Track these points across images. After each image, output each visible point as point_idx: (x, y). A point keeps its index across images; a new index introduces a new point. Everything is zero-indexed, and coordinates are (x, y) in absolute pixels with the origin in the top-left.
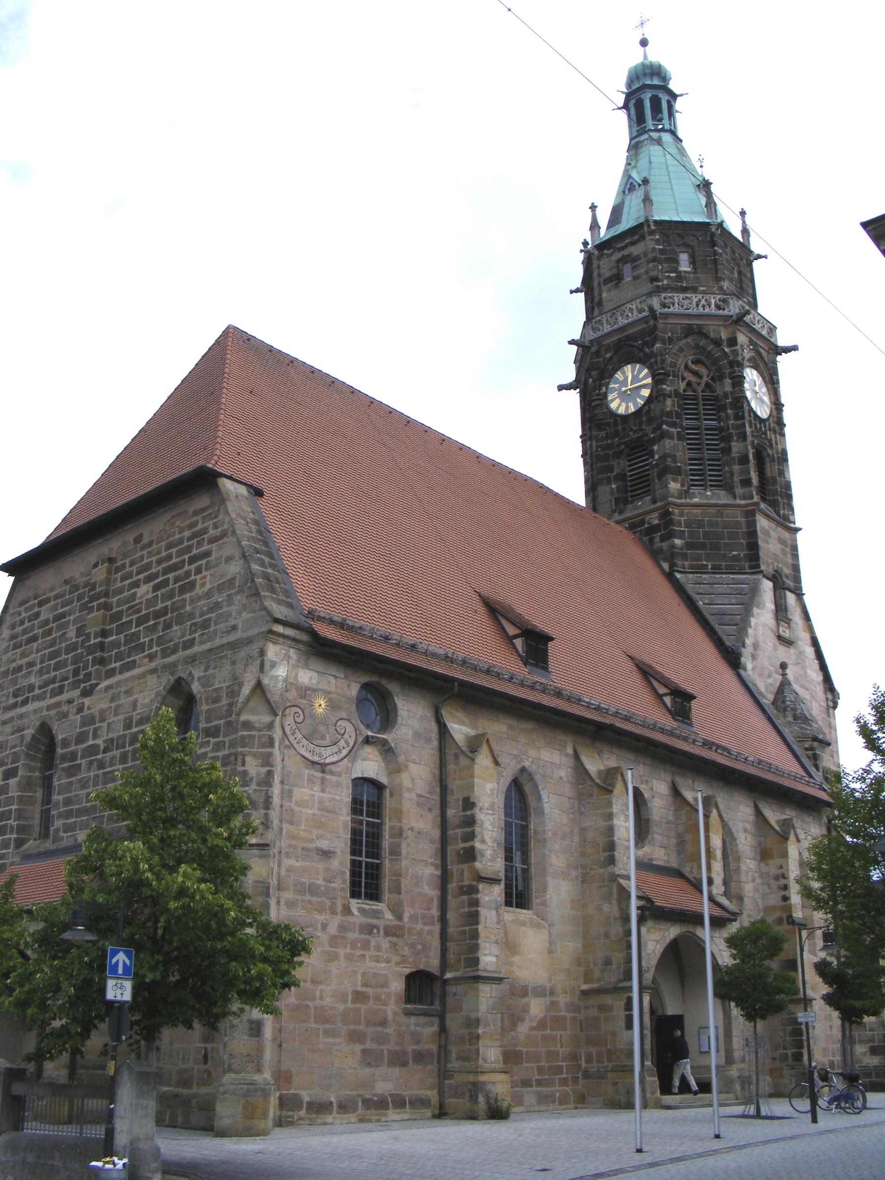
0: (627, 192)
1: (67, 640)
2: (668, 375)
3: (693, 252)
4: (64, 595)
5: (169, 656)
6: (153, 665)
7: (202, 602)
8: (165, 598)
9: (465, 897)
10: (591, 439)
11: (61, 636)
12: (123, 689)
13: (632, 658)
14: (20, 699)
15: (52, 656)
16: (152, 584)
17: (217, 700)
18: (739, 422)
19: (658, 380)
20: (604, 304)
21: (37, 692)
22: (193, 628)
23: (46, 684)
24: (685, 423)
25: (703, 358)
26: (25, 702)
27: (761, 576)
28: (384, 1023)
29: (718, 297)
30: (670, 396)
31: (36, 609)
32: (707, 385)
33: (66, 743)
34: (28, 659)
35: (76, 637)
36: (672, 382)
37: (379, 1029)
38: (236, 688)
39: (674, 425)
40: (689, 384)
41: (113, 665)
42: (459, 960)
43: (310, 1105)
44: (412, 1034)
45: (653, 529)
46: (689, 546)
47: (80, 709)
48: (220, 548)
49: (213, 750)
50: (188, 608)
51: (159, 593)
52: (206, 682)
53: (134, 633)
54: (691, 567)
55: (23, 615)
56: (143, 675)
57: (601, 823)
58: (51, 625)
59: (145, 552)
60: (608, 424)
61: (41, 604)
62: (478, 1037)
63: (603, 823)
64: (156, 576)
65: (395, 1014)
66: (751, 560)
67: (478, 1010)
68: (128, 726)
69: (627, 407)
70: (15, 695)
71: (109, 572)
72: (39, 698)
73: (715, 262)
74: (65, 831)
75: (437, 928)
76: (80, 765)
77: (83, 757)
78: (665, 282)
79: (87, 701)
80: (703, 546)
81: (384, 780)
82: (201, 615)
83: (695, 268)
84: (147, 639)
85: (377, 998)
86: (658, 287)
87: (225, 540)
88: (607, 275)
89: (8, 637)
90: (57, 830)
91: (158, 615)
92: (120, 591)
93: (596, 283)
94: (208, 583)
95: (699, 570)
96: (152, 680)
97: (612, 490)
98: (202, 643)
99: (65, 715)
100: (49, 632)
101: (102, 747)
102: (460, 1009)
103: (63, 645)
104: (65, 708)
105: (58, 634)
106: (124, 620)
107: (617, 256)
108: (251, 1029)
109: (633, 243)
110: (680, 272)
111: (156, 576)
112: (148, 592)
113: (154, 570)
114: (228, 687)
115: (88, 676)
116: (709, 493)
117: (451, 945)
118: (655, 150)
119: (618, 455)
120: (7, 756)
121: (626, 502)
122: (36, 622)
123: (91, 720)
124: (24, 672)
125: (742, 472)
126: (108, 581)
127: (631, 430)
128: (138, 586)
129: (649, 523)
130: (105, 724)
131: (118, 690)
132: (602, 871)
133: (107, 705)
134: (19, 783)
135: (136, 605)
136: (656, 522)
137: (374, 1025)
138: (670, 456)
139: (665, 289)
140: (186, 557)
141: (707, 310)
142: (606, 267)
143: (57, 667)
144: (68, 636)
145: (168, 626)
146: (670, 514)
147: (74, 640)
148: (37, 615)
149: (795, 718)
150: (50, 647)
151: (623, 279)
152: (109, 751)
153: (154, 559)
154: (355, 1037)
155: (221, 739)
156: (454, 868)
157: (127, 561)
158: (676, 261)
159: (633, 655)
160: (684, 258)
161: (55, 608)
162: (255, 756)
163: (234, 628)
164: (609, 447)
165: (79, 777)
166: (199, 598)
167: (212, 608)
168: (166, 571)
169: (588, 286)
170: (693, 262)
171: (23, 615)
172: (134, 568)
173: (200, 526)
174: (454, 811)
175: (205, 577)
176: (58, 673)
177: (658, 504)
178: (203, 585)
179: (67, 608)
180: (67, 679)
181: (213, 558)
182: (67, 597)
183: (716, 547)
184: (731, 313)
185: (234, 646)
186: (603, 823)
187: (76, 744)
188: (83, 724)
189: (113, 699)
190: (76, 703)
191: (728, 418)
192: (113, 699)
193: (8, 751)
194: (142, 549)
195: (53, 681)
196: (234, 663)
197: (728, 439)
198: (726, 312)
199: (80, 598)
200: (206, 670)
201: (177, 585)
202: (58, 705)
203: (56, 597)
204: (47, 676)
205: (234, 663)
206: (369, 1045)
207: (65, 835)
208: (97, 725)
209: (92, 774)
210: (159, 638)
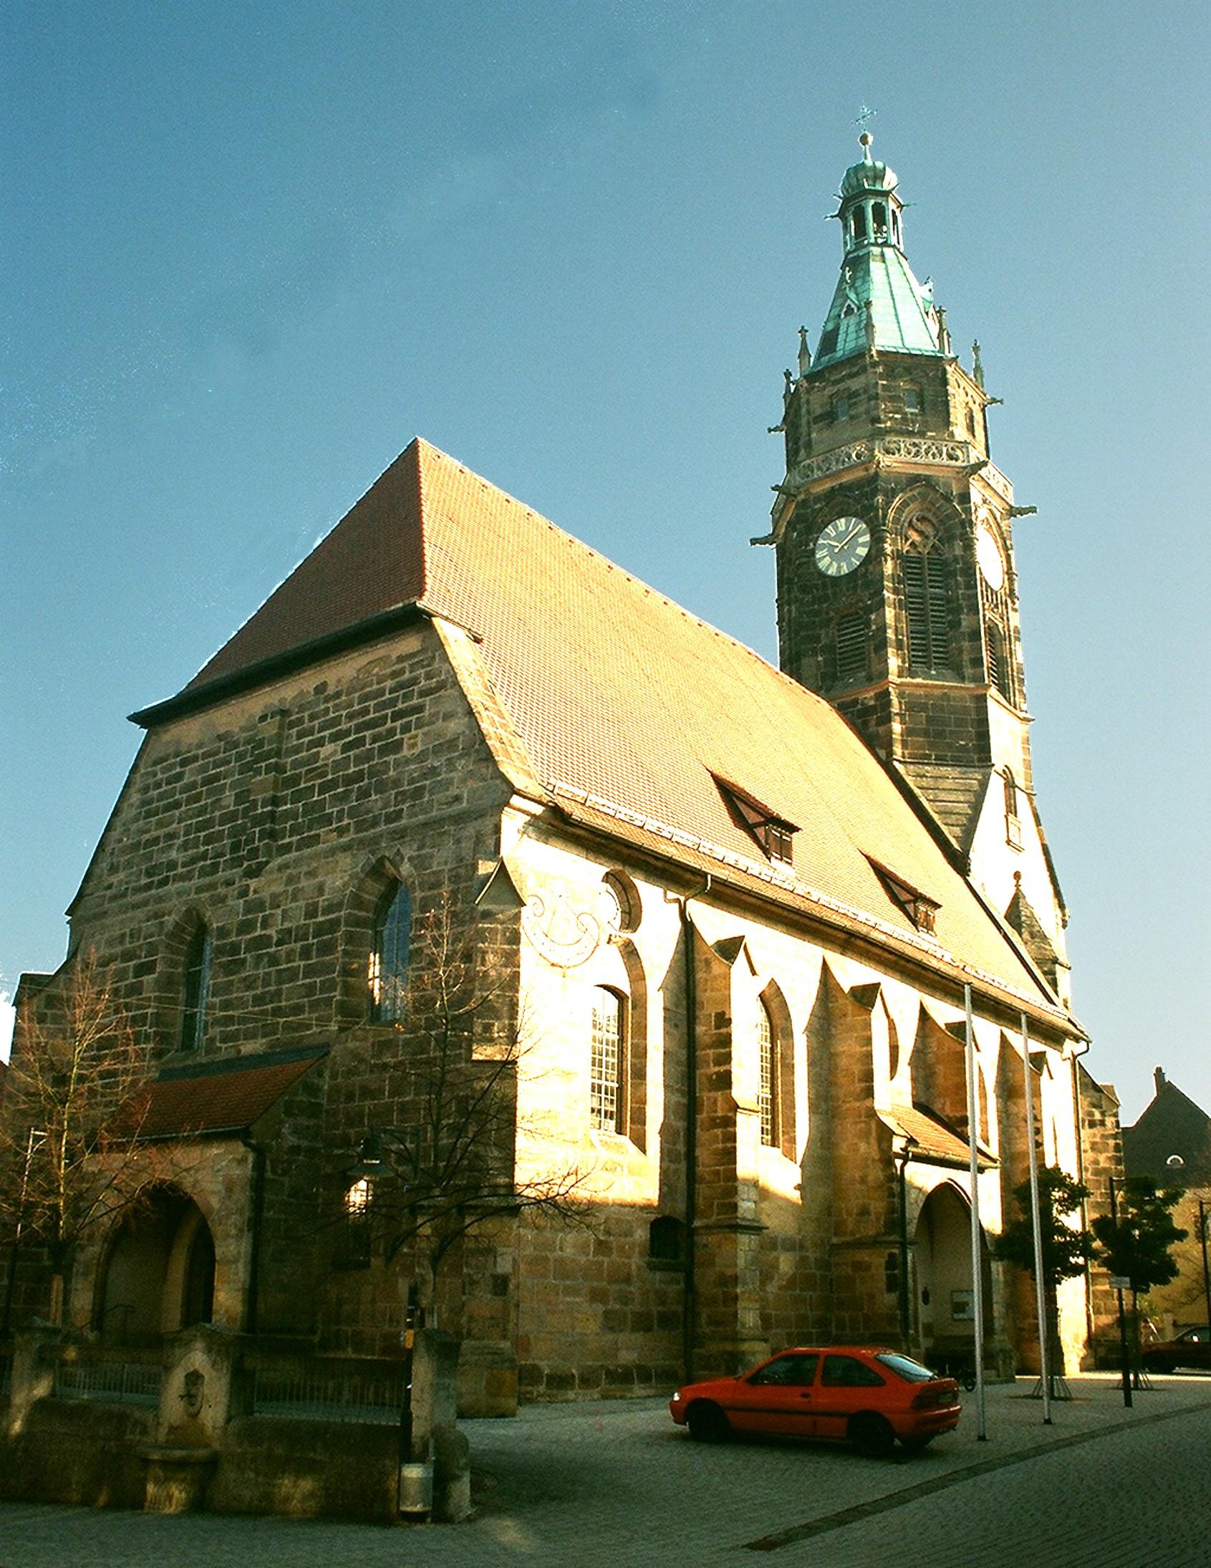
3: (922, 390)
9: (719, 1131)
12: (305, 869)
13: (867, 857)
14: (156, 879)
17: (438, 885)
18: (970, 592)
21: (180, 870)
23: (193, 861)
25: (929, 515)
26: (164, 882)
28: (628, 1280)
31: (178, 770)
33: (222, 933)
34: (166, 830)
37: (623, 1286)
38: (462, 871)
41: (287, 840)
42: (711, 1206)
43: (551, 1378)
44: (656, 1292)
47: (244, 893)
48: (436, 702)
50: (391, 773)
52: (420, 863)
55: (160, 776)
56: (332, 852)
57: (858, 1049)
59: (330, 705)
60: (816, 587)
61: (184, 763)
62: (736, 1298)
63: (858, 1049)
64: (347, 733)
65: (639, 1268)
67: (736, 1265)
68: (311, 912)
69: (839, 567)
70: (149, 874)
71: (281, 727)
72: (182, 878)
74: (223, 1041)
75: (683, 1167)
76: (244, 961)
78: (889, 424)
79: (253, 883)
81: (628, 991)
82: (412, 781)
83: (923, 409)
85: (621, 1249)
88: (819, 411)
90: (212, 1040)
91: (349, 780)
92: (297, 750)
93: (804, 421)
94: (419, 744)
96: (345, 860)
97: (818, 662)
99: (223, 900)
100: (197, 798)
102: (713, 1264)
103: (217, 813)
104: (222, 890)
106: (303, 785)
107: (830, 390)
108: (495, 1286)
109: (851, 376)
110: (906, 414)
111: (347, 733)
113: (344, 727)
115: (254, 853)
117: (702, 1189)
121: (834, 677)
123: (261, 906)
124: (161, 845)
126: (280, 738)
129: (863, 704)
130: (279, 911)
131: (298, 870)
132: (858, 1104)
133: (282, 888)
134: (157, 981)
136: (872, 703)
137: (617, 1281)
139: (888, 432)
140: (389, 711)
141: (937, 460)
142: (817, 402)
144: (223, 803)
145: (364, 794)
147: (232, 808)
148: (179, 777)
149: (1033, 936)
151: (837, 418)
154: (597, 1296)
156: (705, 1095)
157: (306, 714)
159: (871, 854)
161: (204, 769)
162: (495, 952)
164: (817, 613)
168: (359, 728)
169: (791, 423)
171: (160, 776)
172: (316, 722)
173: (407, 675)
174: (704, 1028)
175: (416, 736)
178: (414, 745)
181: (427, 713)
182: (222, 755)
185: (459, 819)
186: (858, 1049)
187: (237, 935)
188: (248, 910)
189: (290, 880)
191: (958, 587)
192: (290, 880)
193: (141, 942)
194: (326, 700)
195: (204, 856)
196: (458, 841)
197: (958, 611)
199: (240, 756)
200: (419, 849)
202: (212, 886)
203: (205, 756)
205: (458, 841)
206: (614, 1306)
207: (224, 1046)
209: (261, 971)
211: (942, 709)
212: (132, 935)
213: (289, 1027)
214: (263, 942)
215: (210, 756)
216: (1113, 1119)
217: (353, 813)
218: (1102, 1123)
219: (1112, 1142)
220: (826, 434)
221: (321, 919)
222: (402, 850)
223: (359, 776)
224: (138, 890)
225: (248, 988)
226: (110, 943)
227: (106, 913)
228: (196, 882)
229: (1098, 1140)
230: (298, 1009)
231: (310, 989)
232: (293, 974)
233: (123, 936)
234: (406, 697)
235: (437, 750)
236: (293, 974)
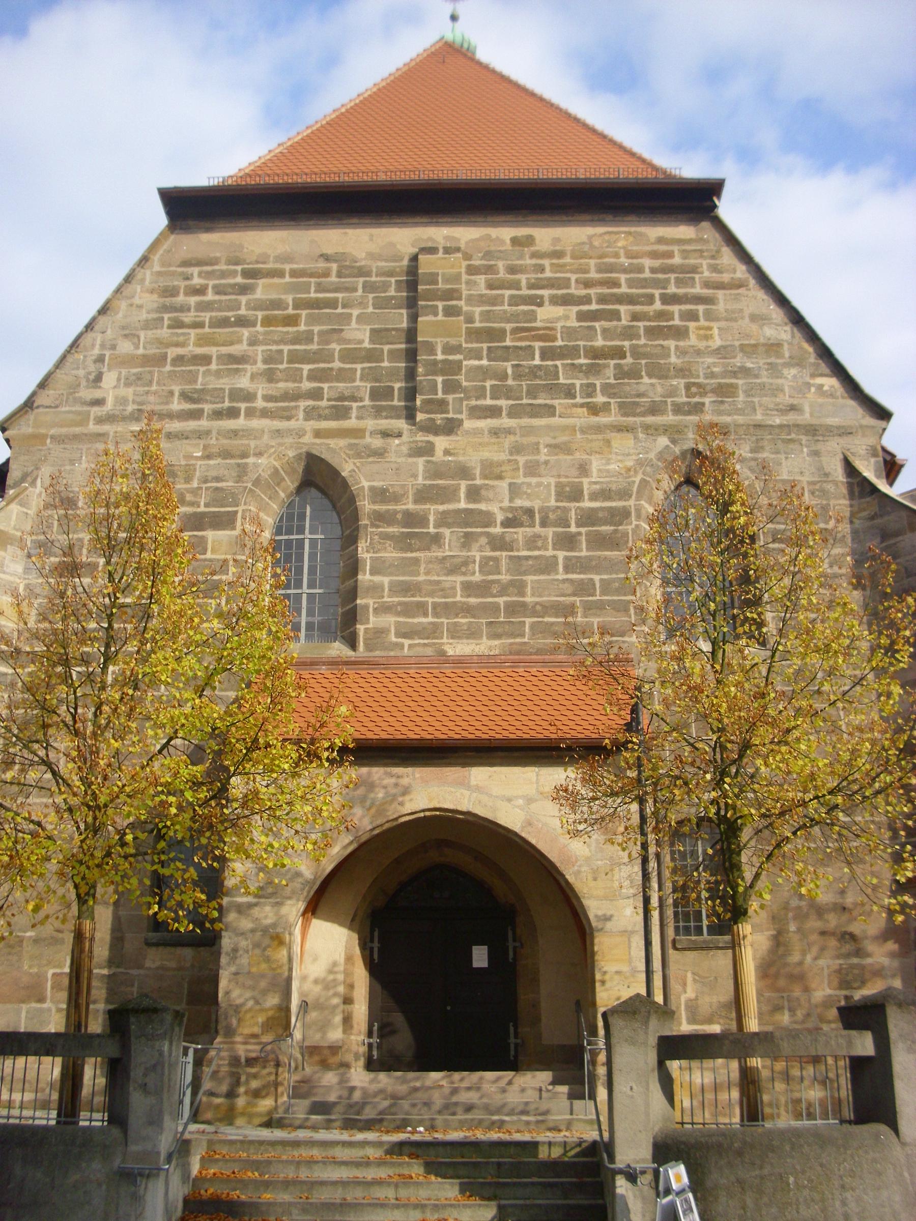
16: (575, 309)
21: (260, 403)
22: (694, 389)
26: (233, 413)
31: (239, 279)
33: (380, 495)
50: (673, 359)
64: (587, 300)
87: (741, 291)
89: (155, 305)
91: (595, 354)
101: (500, 517)
106: (508, 343)
112: (567, 318)
120: (195, 492)
122: (243, 299)
128: (540, 305)
130: (504, 485)
133: (503, 457)
144: (347, 335)
152: (521, 525)
163: (793, 408)
165: (440, 554)
175: (710, 328)
176: (325, 386)
179: (340, 295)
180: (354, 399)
189: (517, 449)
192: (517, 449)
195: (316, 394)
204: (291, 385)
221: (587, 504)
236: (549, 566)
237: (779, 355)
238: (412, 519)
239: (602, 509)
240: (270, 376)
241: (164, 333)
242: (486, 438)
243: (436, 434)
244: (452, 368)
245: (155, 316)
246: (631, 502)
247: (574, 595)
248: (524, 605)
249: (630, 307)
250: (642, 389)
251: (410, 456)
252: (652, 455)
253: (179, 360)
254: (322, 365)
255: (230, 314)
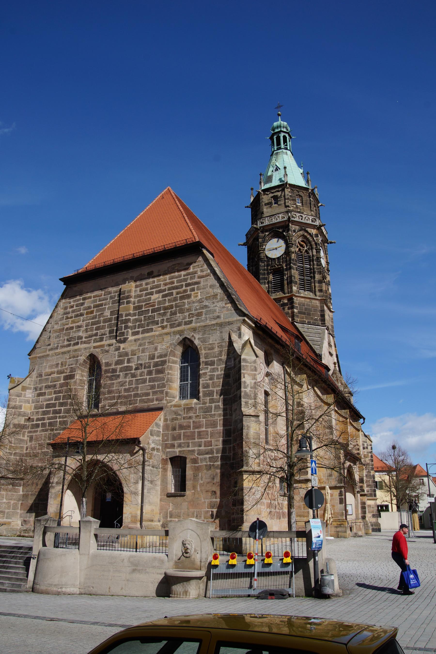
0: (274, 171)
1: (104, 316)
2: (293, 245)
4: (101, 296)
5: (176, 327)
6: (165, 331)
7: (196, 304)
8: (170, 301)
10: (252, 266)
11: (99, 315)
12: (148, 341)
14: (72, 342)
15: (93, 324)
16: (161, 294)
17: (213, 348)
19: (288, 246)
20: (265, 213)
21: (84, 339)
22: (191, 316)
23: (91, 336)
24: (298, 264)
26: (77, 344)
27: (325, 327)
29: (312, 217)
30: (293, 253)
31: (82, 301)
32: (306, 251)
33: (107, 364)
35: (110, 315)
36: (294, 248)
39: (295, 264)
40: (300, 249)
45: (284, 305)
46: (300, 313)
47: (118, 349)
49: (210, 372)
50: (186, 306)
51: (167, 298)
52: (203, 341)
53: (150, 316)
54: (300, 320)
56: (160, 335)
58: (92, 309)
60: (265, 261)
64: (165, 290)
66: (322, 321)
68: (152, 357)
70: (68, 340)
72: (85, 343)
73: (310, 203)
76: (119, 375)
77: (121, 371)
78: (292, 208)
79: (122, 346)
80: (304, 313)
84: (160, 319)
86: (289, 209)
88: (267, 202)
89: (63, 313)
91: (165, 308)
95: (303, 323)
96: (167, 338)
98: (196, 322)
101: (134, 367)
103: (102, 319)
104: (107, 348)
105: (98, 314)
106: (143, 309)
110: (297, 205)
111: (165, 290)
112: (159, 297)
114: (218, 343)
115: (123, 334)
116: (306, 293)
118: (285, 156)
119: (268, 274)
120: (66, 369)
122: (82, 307)
124: (74, 330)
125: (319, 286)
127: (276, 264)
128: (152, 295)
129: (283, 302)
130: (136, 357)
131: (144, 341)
133: (137, 348)
135: (151, 303)
138: (293, 276)
140: (184, 283)
141: (308, 222)
143: (97, 329)
144: (104, 314)
146: (293, 299)
147: (109, 317)
148: (82, 304)
150: (92, 319)
152: (139, 369)
153: (162, 283)
155: (215, 366)
158: (295, 200)
160: (298, 200)
161: (95, 301)
163: (218, 317)
165: (119, 381)
166: (194, 302)
167: (203, 307)
168: (169, 289)
170: (302, 203)
171: (72, 303)
172: (149, 286)
175: (197, 293)
176: (98, 331)
177: (287, 295)
178: (196, 296)
179: (104, 302)
180: (105, 334)
181: (202, 284)
182: (103, 297)
183: (309, 314)
184: (317, 224)
185: (221, 325)
187: (115, 365)
188: (120, 356)
189: (140, 345)
190: (114, 346)
192: (140, 345)
195: (96, 335)
197: (314, 273)
198: (315, 224)
201: (178, 296)
204: (91, 332)
205: (221, 332)
208: (130, 357)
210: (167, 319)
211: (309, 305)
212: (62, 364)
213: (142, 401)
214: (129, 368)
215: (98, 297)
216: (370, 447)
217: (168, 320)
218: (367, 448)
219: (370, 454)
220: (269, 210)
221: (156, 360)
222: (195, 335)
223: (171, 307)
224: (63, 347)
225: (122, 386)
226: (51, 367)
227: (48, 355)
228: (93, 344)
229: (366, 453)
230: (148, 394)
231: (153, 387)
232: (144, 381)
233: (58, 364)
234: (191, 278)
235: (207, 299)
236: (144, 381)
237: (216, 299)
238: (114, 371)
239: (159, 361)
240: (86, 331)
241: (64, 321)
242: (133, 343)
243: (121, 343)
244: (128, 321)
245: (62, 316)
246: (167, 358)
247: (150, 389)
248: (138, 394)
249: (176, 290)
250: (177, 318)
251: (115, 351)
252: (174, 341)
253: (67, 329)
254: (98, 325)
255: (78, 313)
